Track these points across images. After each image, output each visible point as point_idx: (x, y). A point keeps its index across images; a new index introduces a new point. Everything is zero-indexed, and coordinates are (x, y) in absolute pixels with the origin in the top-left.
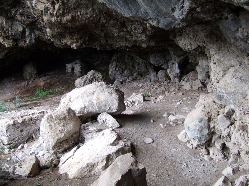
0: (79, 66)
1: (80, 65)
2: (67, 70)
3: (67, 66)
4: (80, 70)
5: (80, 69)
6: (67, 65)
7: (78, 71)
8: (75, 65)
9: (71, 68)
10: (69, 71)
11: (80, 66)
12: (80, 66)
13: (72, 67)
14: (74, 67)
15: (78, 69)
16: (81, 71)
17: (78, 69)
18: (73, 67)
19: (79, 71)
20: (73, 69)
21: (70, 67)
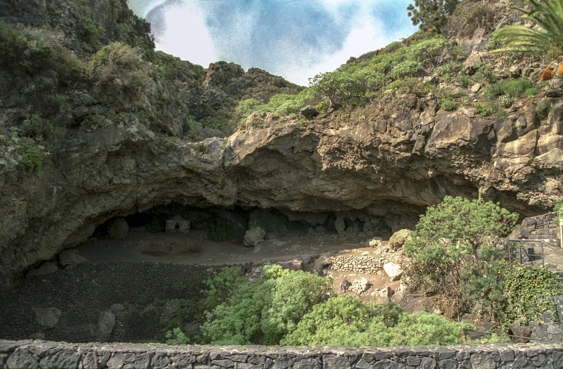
4: (189, 227)
5: (188, 225)
15: (185, 225)
20: (177, 227)
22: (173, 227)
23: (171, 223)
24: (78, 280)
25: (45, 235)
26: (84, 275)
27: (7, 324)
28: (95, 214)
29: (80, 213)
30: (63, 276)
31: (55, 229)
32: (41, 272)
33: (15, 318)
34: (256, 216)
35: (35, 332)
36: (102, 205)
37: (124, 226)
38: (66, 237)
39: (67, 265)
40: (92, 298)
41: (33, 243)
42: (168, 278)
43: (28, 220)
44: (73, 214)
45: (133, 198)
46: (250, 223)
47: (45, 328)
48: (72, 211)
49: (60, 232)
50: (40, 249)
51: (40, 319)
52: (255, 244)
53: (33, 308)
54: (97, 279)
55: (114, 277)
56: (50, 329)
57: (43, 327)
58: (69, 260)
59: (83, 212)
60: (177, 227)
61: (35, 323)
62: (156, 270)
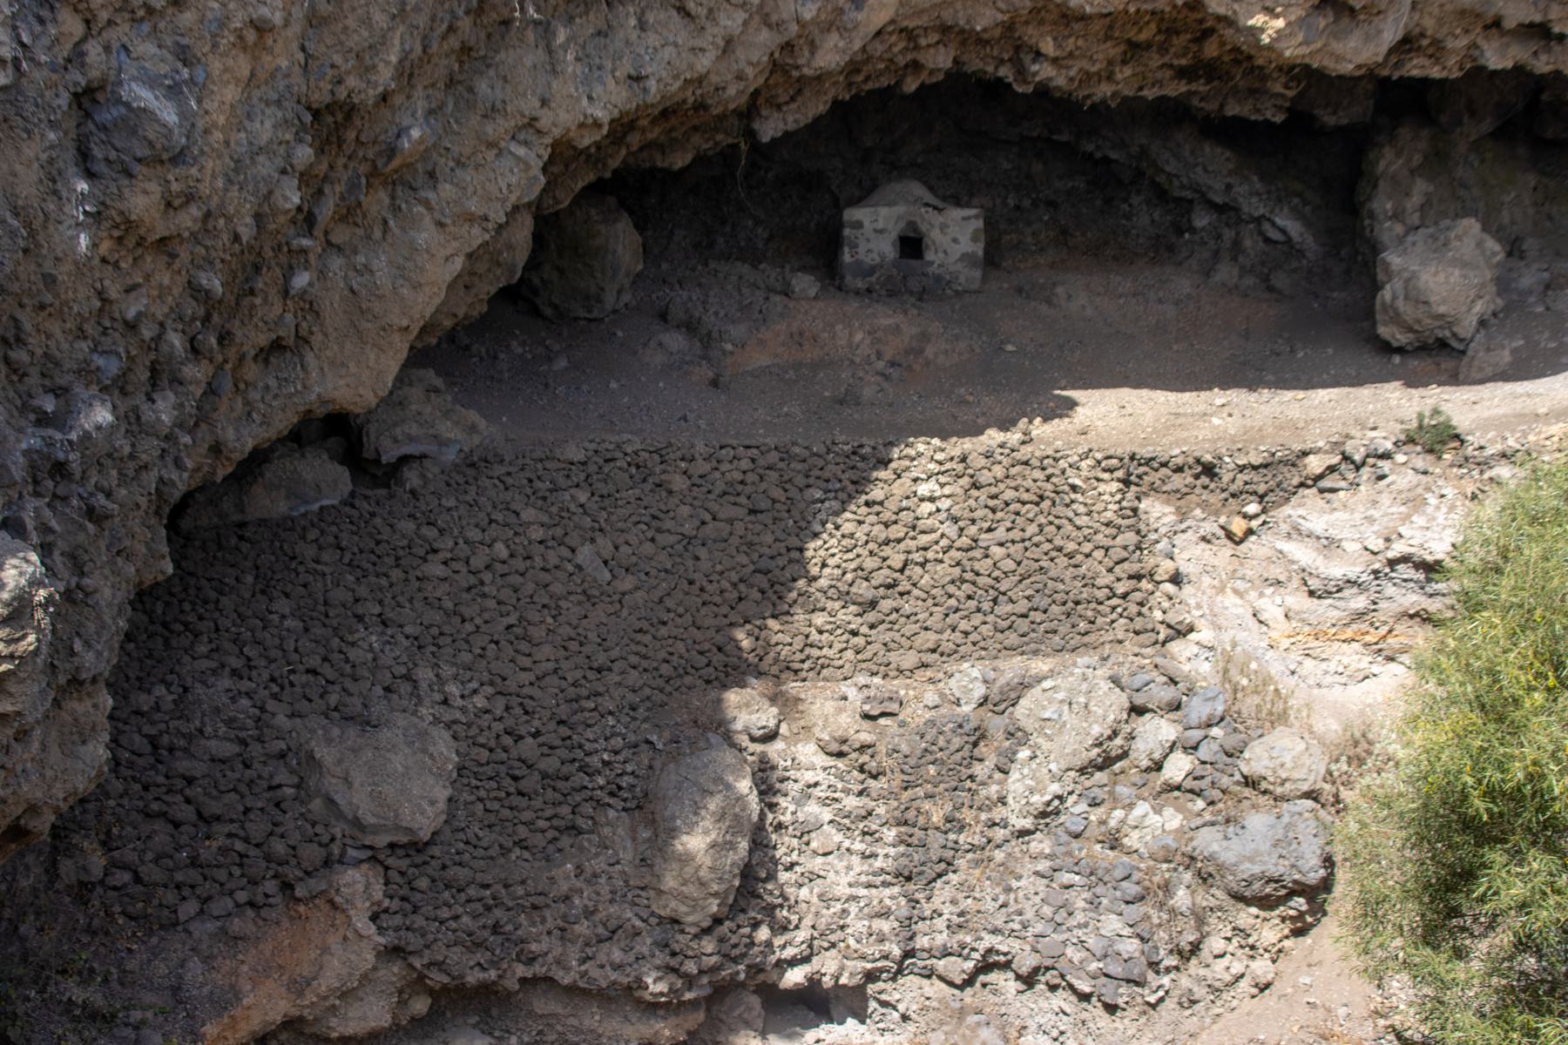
0: (964, 219)
1: (973, 212)
2: (856, 246)
3: (858, 225)
4: (979, 248)
5: (975, 239)
6: (852, 214)
7: (958, 256)
8: (931, 215)
9: (894, 235)
10: (871, 259)
11: (976, 217)
12: (976, 217)
13: (902, 225)
14: (923, 228)
15: (955, 235)
16: (980, 253)
17: (955, 241)
18: (912, 225)
19: (964, 257)
20: (912, 245)
21: (880, 225)
22: (885, 248)
23: (873, 228)
24: (501, 550)
25: (339, 249)
26: (528, 514)
27: (149, 815)
28: (597, 124)
29: (531, 105)
30: (408, 526)
31: (396, 209)
32: (267, 503)
33: (190, 781)
34: (1417, 159)
35: (327, 863)
36: (626, 67)
37: (622, 241)
38: (458, 264)
39: (405, 459)
40: (601, 659)
41: (286, 293)
42: (1000, 533)
43: (308, 118)
44: (492, 112)
45: (777, 26)
46: (1382, 204)
47: (382, 840)
48: (483, 87)
49: (425, 235)
50: (317, 339)
51: (347, 780)
52: (1467, 326)
53: (281, 720)
54: (605, 545)
55: (688, 528)
56: (416, 847)
57: (376, 830)
58: (414, 430)
59: (544, 102)
60: (912, 245)
61: (317, 805)
62: (924, 489)
